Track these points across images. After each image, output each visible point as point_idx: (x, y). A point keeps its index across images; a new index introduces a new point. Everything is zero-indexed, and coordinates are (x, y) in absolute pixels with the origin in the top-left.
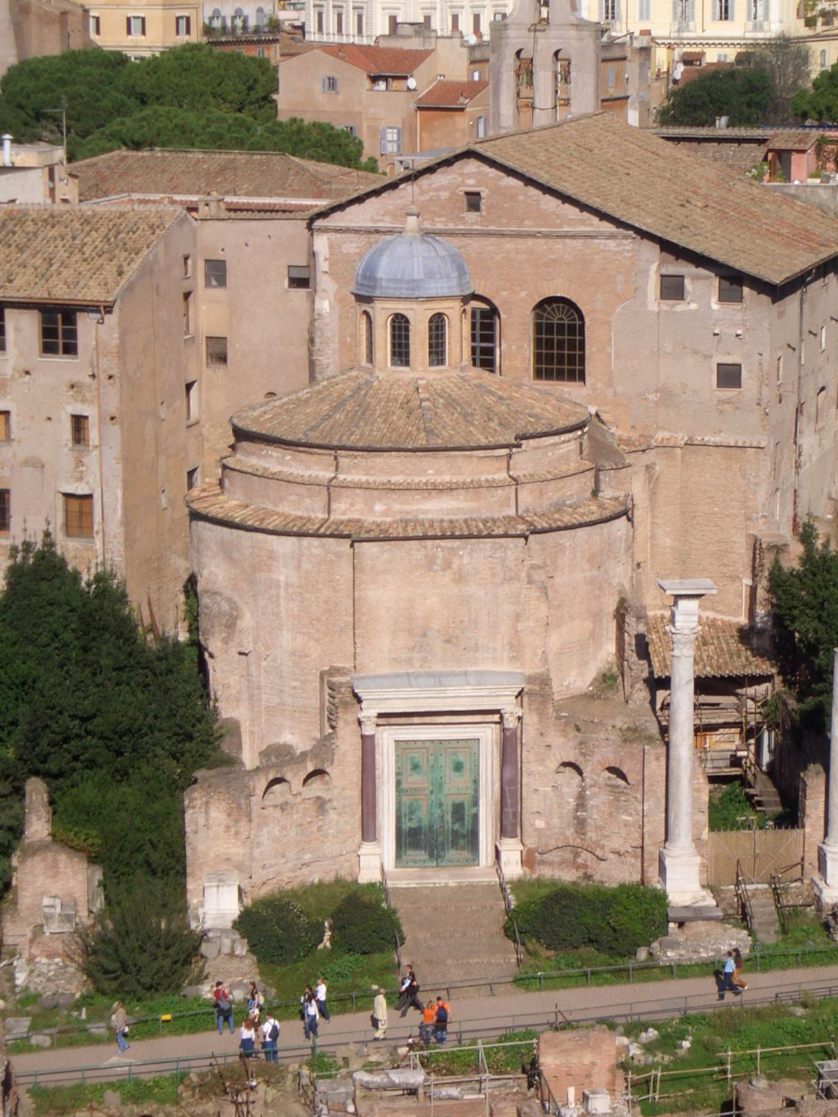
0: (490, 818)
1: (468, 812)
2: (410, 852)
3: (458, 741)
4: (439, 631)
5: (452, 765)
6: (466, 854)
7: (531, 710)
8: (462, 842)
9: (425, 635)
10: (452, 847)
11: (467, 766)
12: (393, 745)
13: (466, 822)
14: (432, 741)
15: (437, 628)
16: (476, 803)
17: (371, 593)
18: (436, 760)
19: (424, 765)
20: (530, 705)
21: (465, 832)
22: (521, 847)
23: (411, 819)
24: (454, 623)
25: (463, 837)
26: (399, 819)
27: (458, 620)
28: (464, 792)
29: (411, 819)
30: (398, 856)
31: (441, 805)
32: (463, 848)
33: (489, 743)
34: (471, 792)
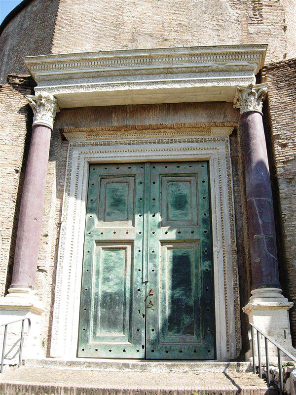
0: (230, 274)
1: (197, 269)
2: (102, 333)
3: (179, 163)
4: (151, 35)
5: (171, 200)
6: (193, 340)
7: (279, 88)
8: (187, 320)
9: (134, 40)
10: (170, 329)
11: (192, 201)
12: (84, 169)
13: (193, 286)
14: (141, 164)
15: (148, 32)
16: (209, 255)
17: (76, 7)
18: (147, 190)
19: (129, 199)
20: (276, 83)
21: (191, 303)
22: (285, 301)
23: (106, 280)
24: (169, 26)
25: (189, 310)
26: (86, 275)
27: (175, 24)
28: (189, 236)
29: (106, 280)
30: (82, 339)
31: (153, 256)
32: (189, 331)
33: (223, 162)
34: (199, 235)
